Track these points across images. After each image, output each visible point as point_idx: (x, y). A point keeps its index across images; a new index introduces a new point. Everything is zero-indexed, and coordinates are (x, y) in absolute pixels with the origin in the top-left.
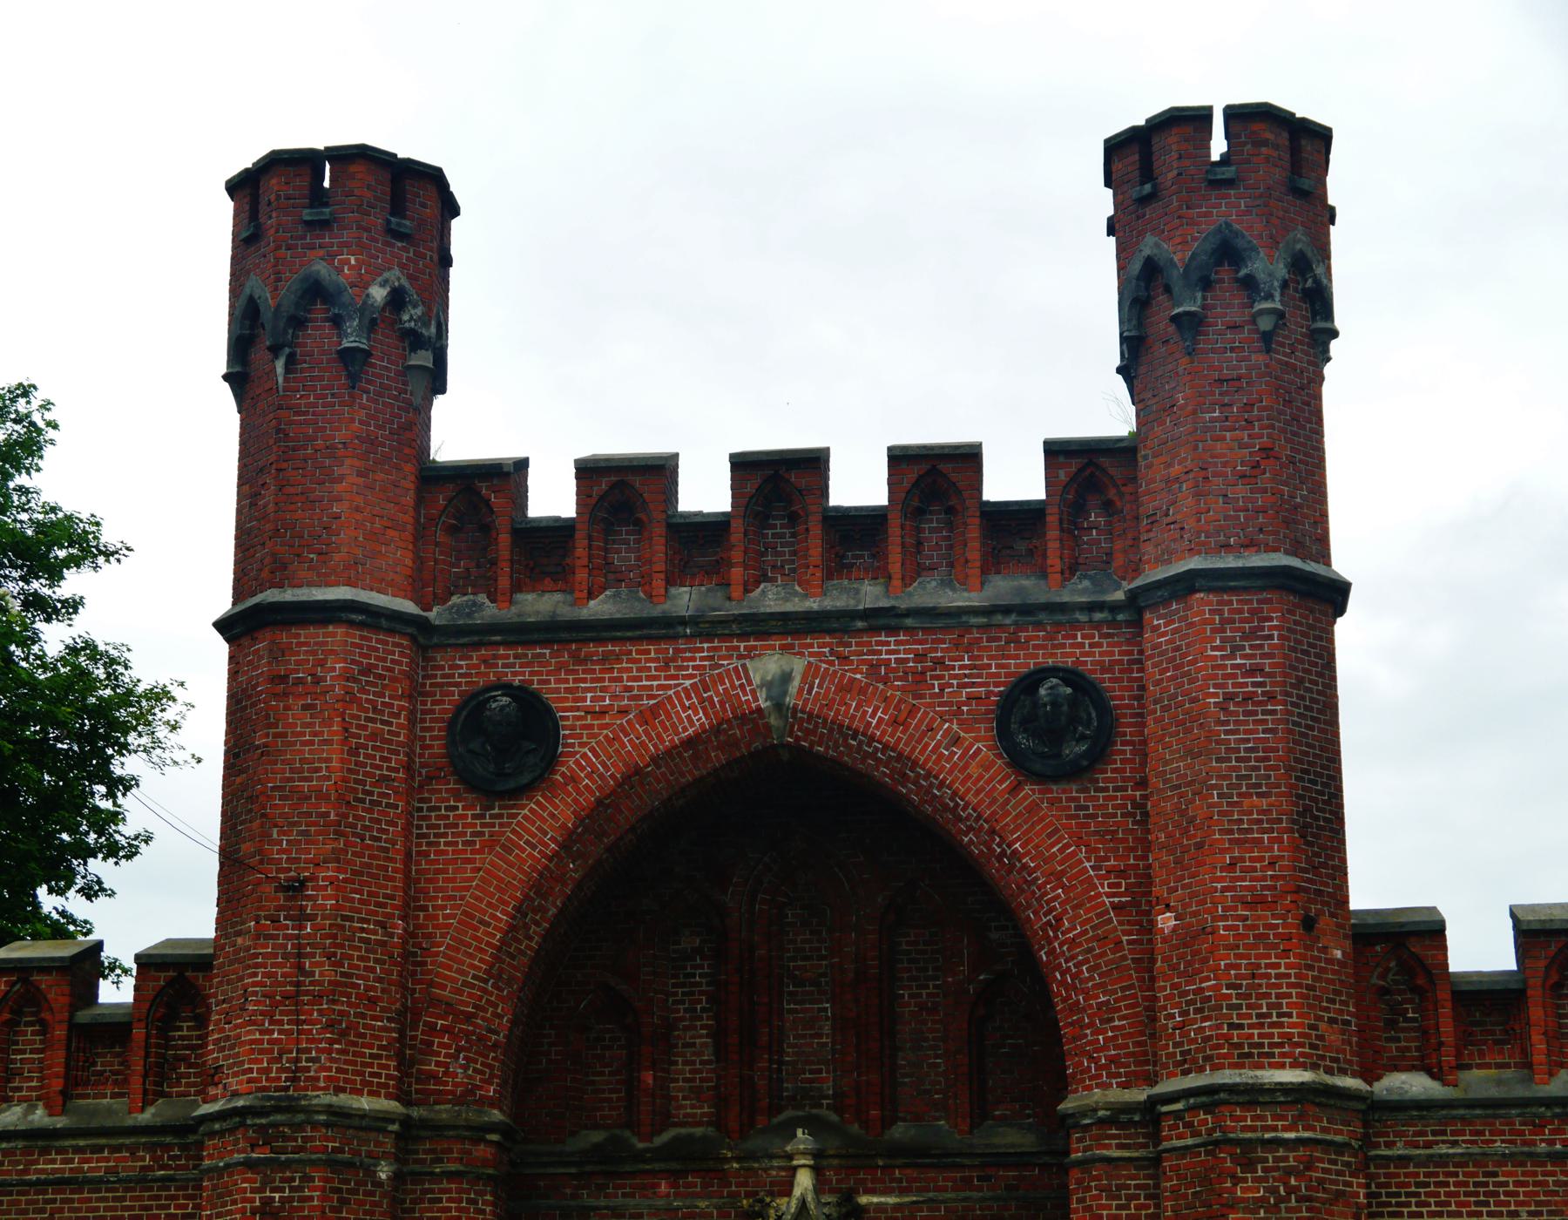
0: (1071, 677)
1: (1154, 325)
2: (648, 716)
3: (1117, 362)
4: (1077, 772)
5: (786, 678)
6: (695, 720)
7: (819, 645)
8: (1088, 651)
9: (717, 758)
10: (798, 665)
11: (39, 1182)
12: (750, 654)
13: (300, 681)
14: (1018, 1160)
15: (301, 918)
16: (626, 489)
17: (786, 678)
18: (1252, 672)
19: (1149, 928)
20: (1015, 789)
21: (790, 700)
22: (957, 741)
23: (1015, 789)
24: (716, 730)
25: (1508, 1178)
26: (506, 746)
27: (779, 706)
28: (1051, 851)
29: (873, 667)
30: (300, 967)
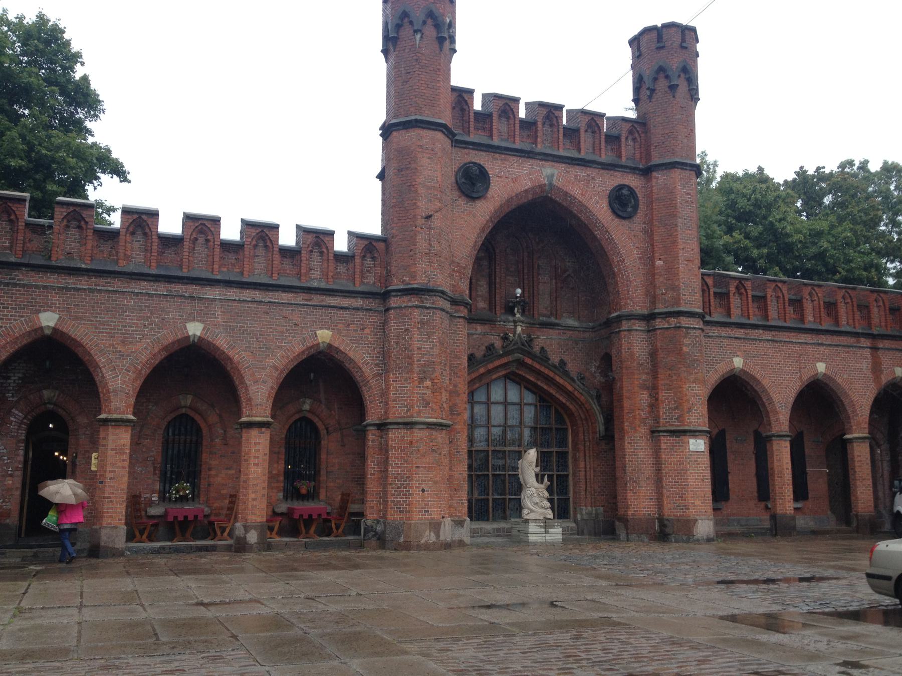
0: (630, 189)
1: (642, 89)
2: (515, 180)
3: (632, 98)
4: (628, 217)
5: (553, 175)
6: (527, 184)
7: (562, 167)
8: (633, 181)
9: (530, 197)
10: (556, 172)
11: (325, 306)
12: (543, 166)
13: (427, 149)
14: (573, 329)
15: (430, 228)
16: (505, 105)
17: (553, 175)
18: (688, 194)
19: (653, 265)
20: (613, 220)
21: (554, 182)
22: (598, 202)
23: (613, 220)
24: (533, 188)
25: (726, 342)
26: (472, 183)
27: (551, 184)
28: (624, 240)
29: (576, 176)
30: (430, 245)
